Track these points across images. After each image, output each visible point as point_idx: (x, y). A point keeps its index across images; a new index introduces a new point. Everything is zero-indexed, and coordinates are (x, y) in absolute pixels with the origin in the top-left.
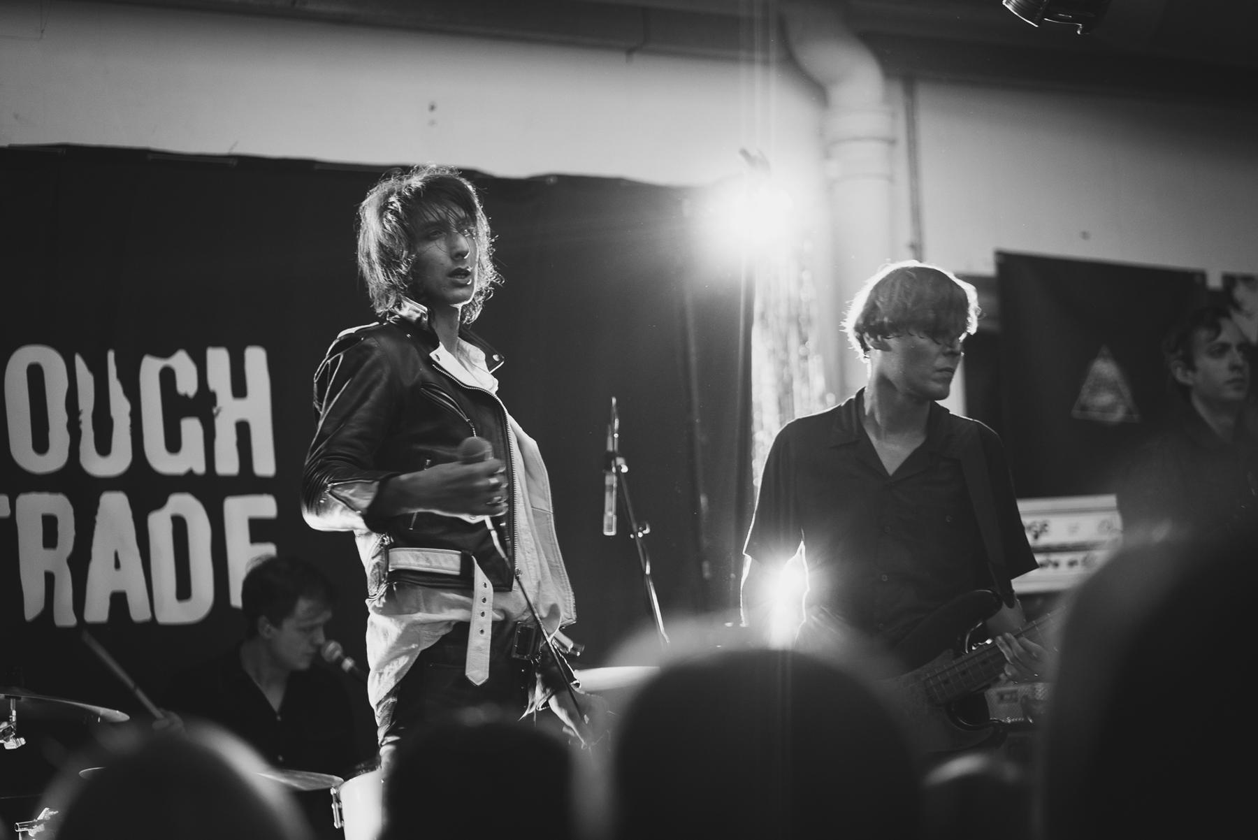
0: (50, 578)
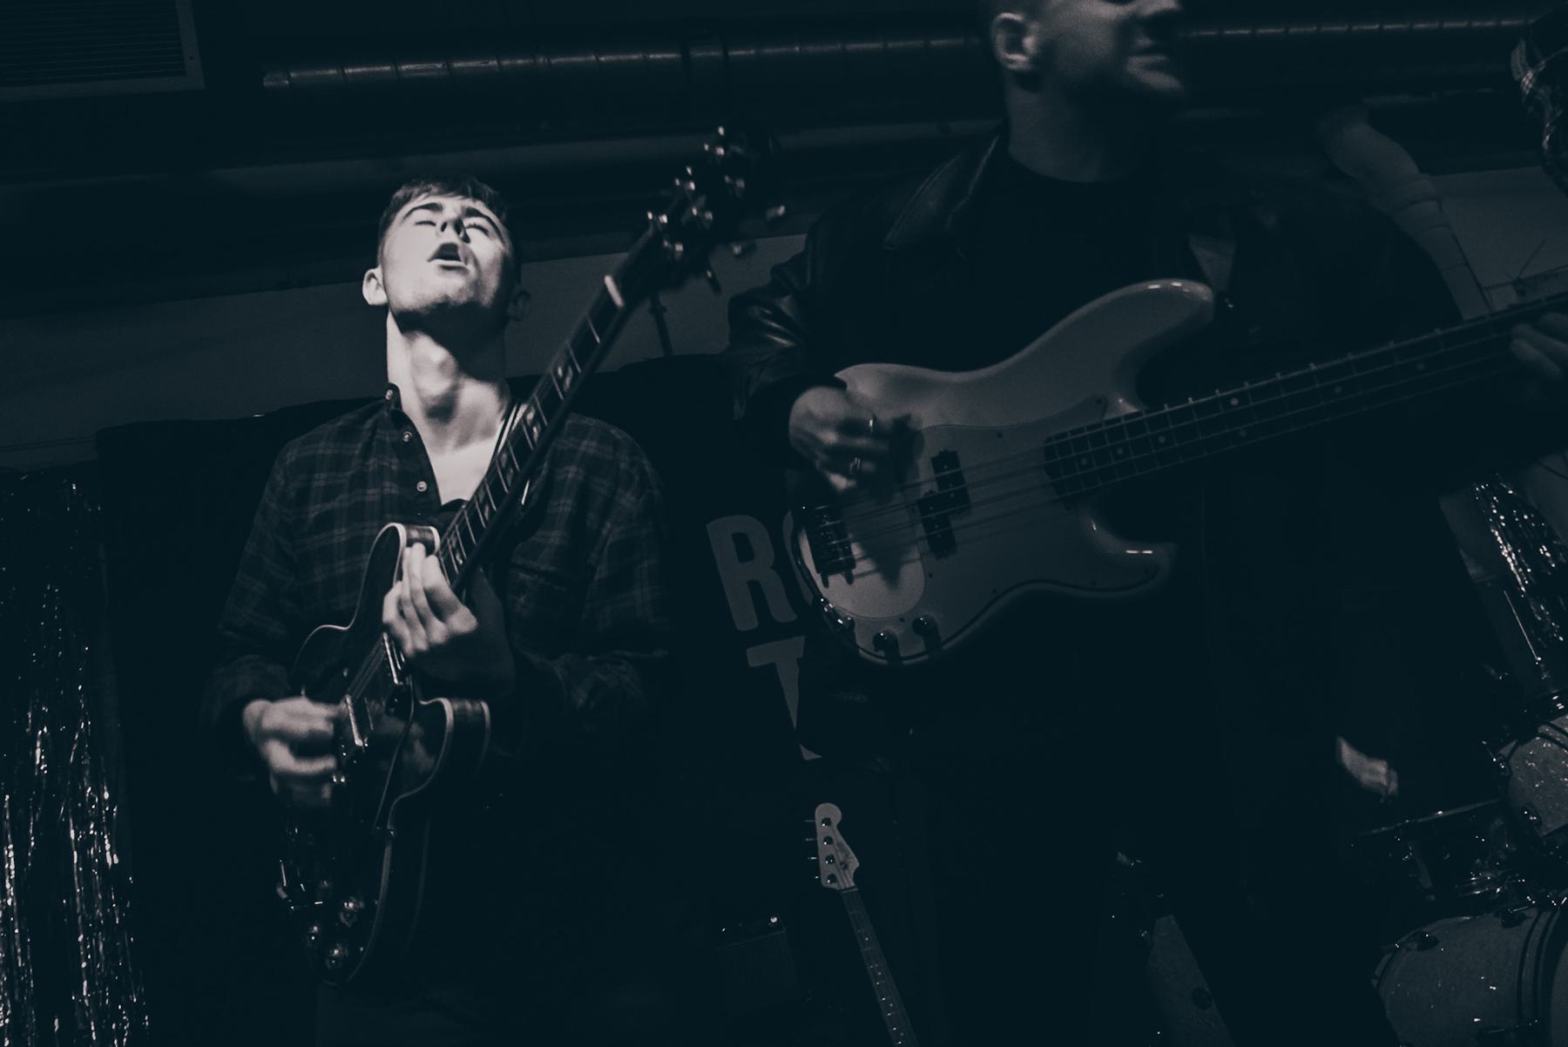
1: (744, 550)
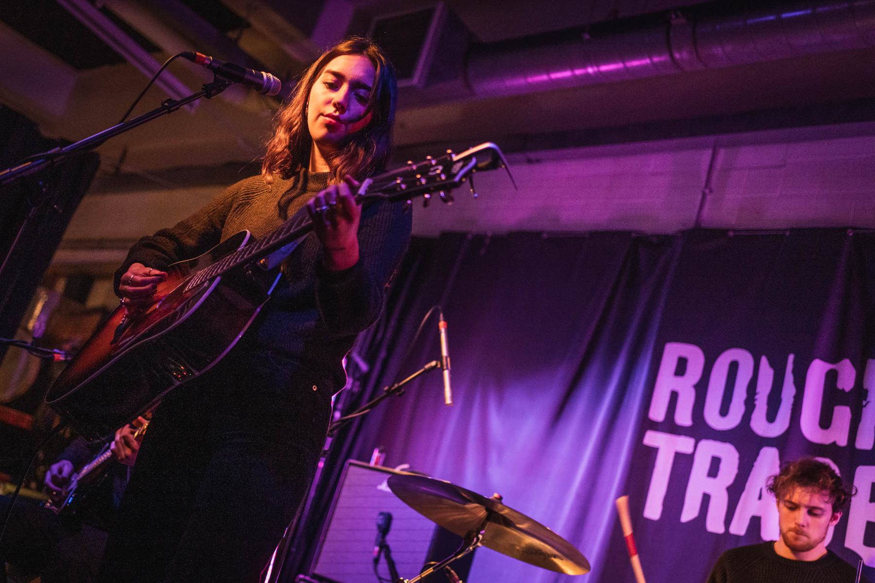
0: (706, 499)
1: (681, 368)
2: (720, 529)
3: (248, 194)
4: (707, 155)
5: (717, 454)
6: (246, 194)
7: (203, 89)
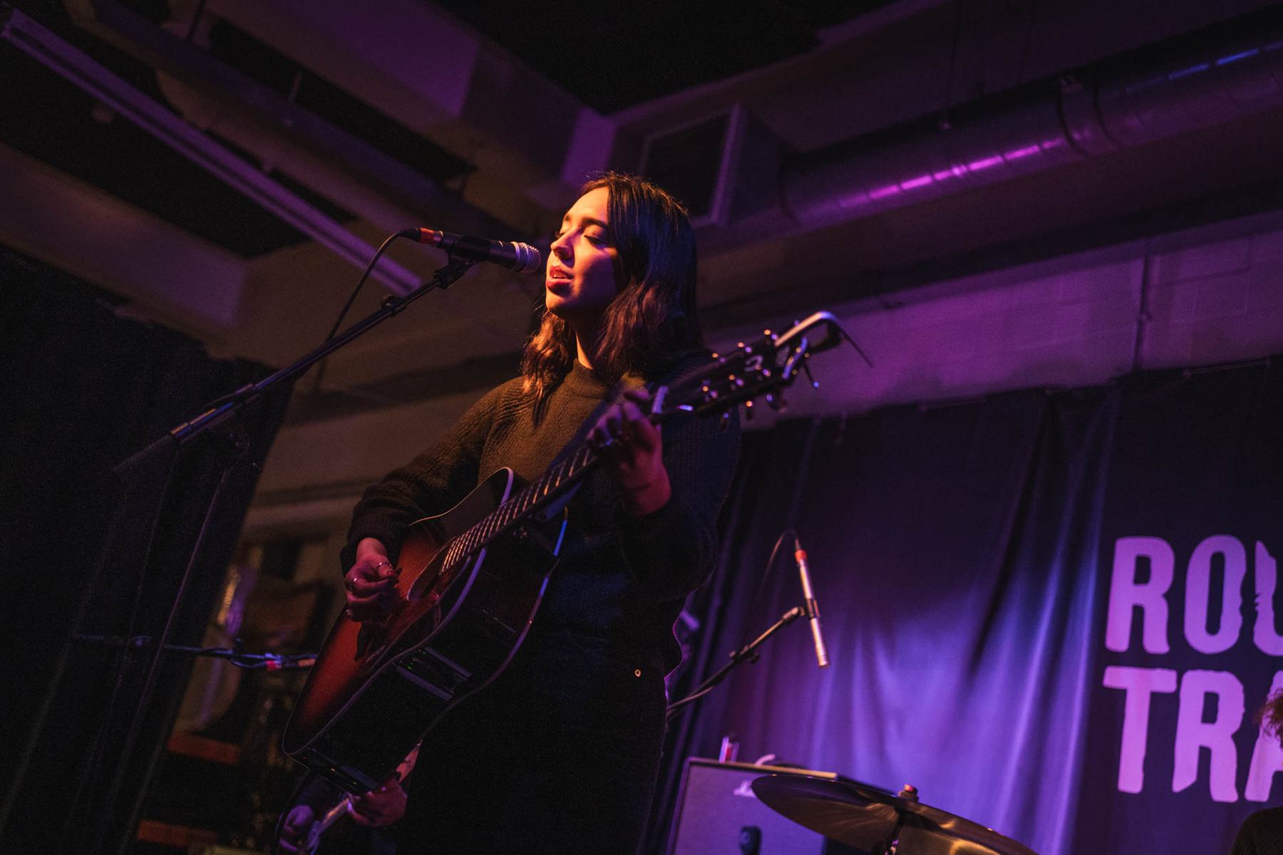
0: (1205, 755)
1: (1143, 573)
2: (1232, 796)
3: (511, 408)
4: (1137, 268)
5: (1211, 689)
6: (506, 409)
7: (435, 277)
